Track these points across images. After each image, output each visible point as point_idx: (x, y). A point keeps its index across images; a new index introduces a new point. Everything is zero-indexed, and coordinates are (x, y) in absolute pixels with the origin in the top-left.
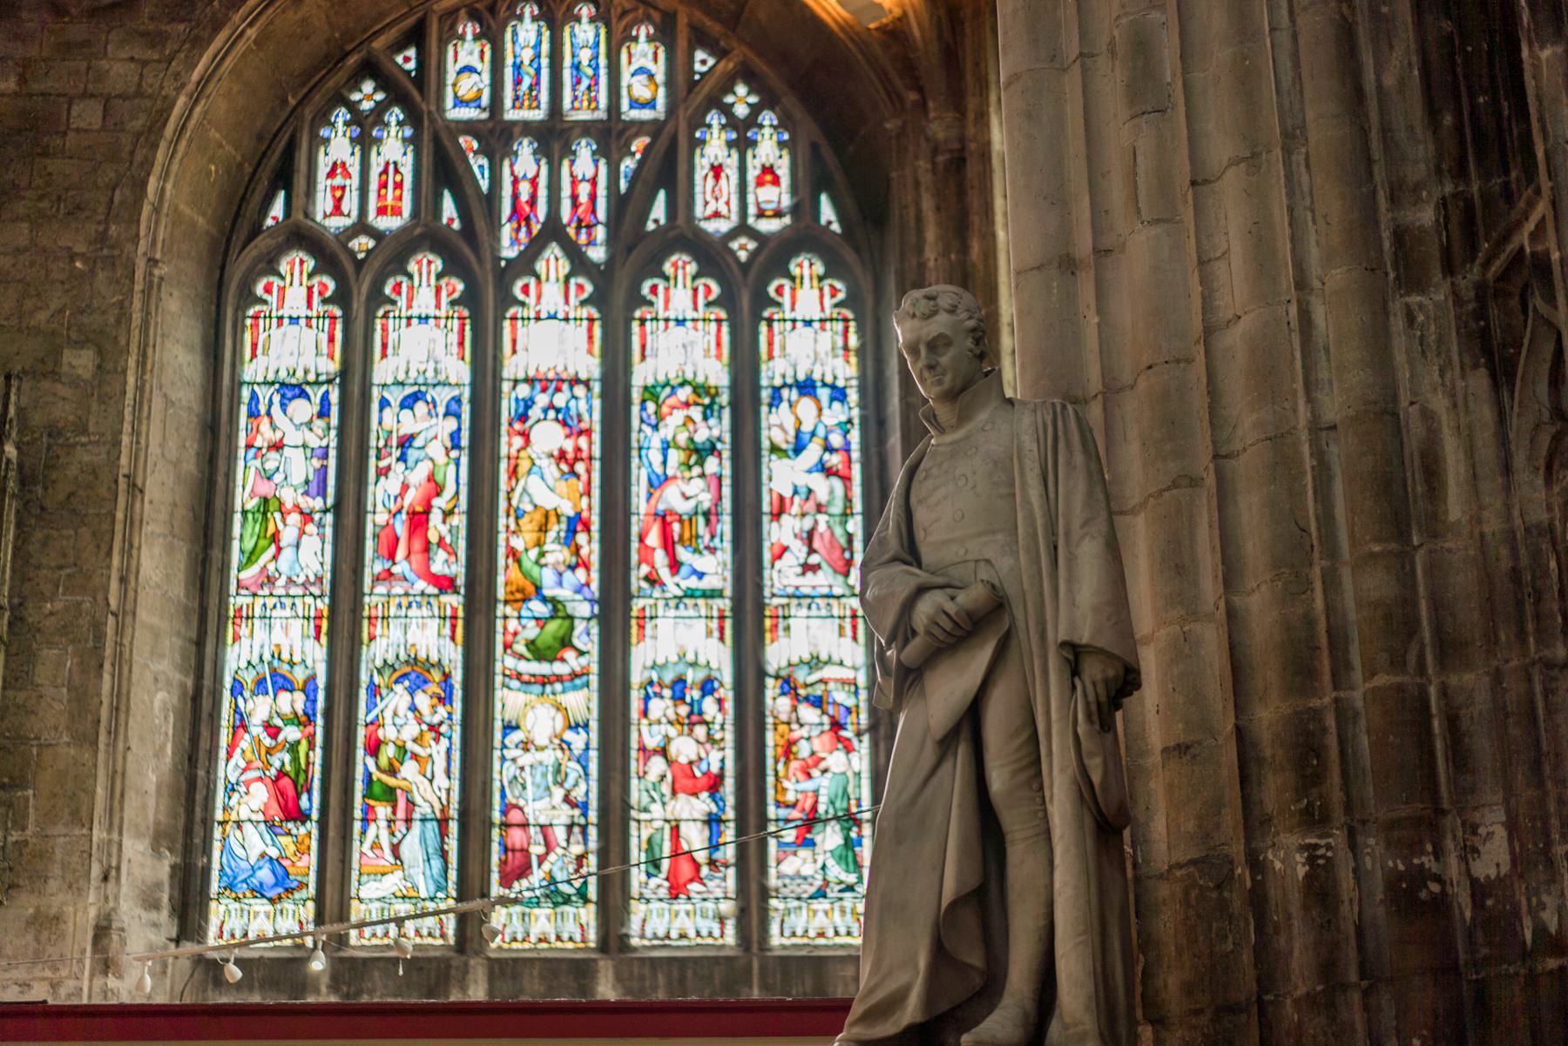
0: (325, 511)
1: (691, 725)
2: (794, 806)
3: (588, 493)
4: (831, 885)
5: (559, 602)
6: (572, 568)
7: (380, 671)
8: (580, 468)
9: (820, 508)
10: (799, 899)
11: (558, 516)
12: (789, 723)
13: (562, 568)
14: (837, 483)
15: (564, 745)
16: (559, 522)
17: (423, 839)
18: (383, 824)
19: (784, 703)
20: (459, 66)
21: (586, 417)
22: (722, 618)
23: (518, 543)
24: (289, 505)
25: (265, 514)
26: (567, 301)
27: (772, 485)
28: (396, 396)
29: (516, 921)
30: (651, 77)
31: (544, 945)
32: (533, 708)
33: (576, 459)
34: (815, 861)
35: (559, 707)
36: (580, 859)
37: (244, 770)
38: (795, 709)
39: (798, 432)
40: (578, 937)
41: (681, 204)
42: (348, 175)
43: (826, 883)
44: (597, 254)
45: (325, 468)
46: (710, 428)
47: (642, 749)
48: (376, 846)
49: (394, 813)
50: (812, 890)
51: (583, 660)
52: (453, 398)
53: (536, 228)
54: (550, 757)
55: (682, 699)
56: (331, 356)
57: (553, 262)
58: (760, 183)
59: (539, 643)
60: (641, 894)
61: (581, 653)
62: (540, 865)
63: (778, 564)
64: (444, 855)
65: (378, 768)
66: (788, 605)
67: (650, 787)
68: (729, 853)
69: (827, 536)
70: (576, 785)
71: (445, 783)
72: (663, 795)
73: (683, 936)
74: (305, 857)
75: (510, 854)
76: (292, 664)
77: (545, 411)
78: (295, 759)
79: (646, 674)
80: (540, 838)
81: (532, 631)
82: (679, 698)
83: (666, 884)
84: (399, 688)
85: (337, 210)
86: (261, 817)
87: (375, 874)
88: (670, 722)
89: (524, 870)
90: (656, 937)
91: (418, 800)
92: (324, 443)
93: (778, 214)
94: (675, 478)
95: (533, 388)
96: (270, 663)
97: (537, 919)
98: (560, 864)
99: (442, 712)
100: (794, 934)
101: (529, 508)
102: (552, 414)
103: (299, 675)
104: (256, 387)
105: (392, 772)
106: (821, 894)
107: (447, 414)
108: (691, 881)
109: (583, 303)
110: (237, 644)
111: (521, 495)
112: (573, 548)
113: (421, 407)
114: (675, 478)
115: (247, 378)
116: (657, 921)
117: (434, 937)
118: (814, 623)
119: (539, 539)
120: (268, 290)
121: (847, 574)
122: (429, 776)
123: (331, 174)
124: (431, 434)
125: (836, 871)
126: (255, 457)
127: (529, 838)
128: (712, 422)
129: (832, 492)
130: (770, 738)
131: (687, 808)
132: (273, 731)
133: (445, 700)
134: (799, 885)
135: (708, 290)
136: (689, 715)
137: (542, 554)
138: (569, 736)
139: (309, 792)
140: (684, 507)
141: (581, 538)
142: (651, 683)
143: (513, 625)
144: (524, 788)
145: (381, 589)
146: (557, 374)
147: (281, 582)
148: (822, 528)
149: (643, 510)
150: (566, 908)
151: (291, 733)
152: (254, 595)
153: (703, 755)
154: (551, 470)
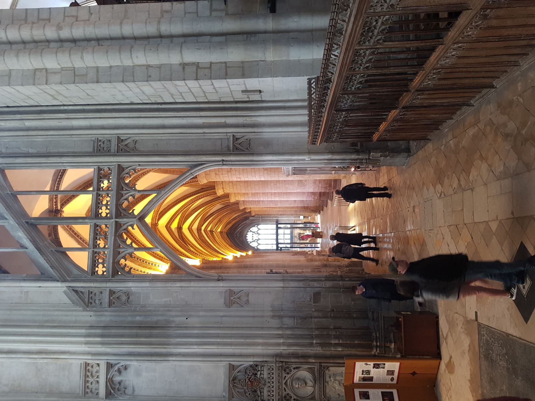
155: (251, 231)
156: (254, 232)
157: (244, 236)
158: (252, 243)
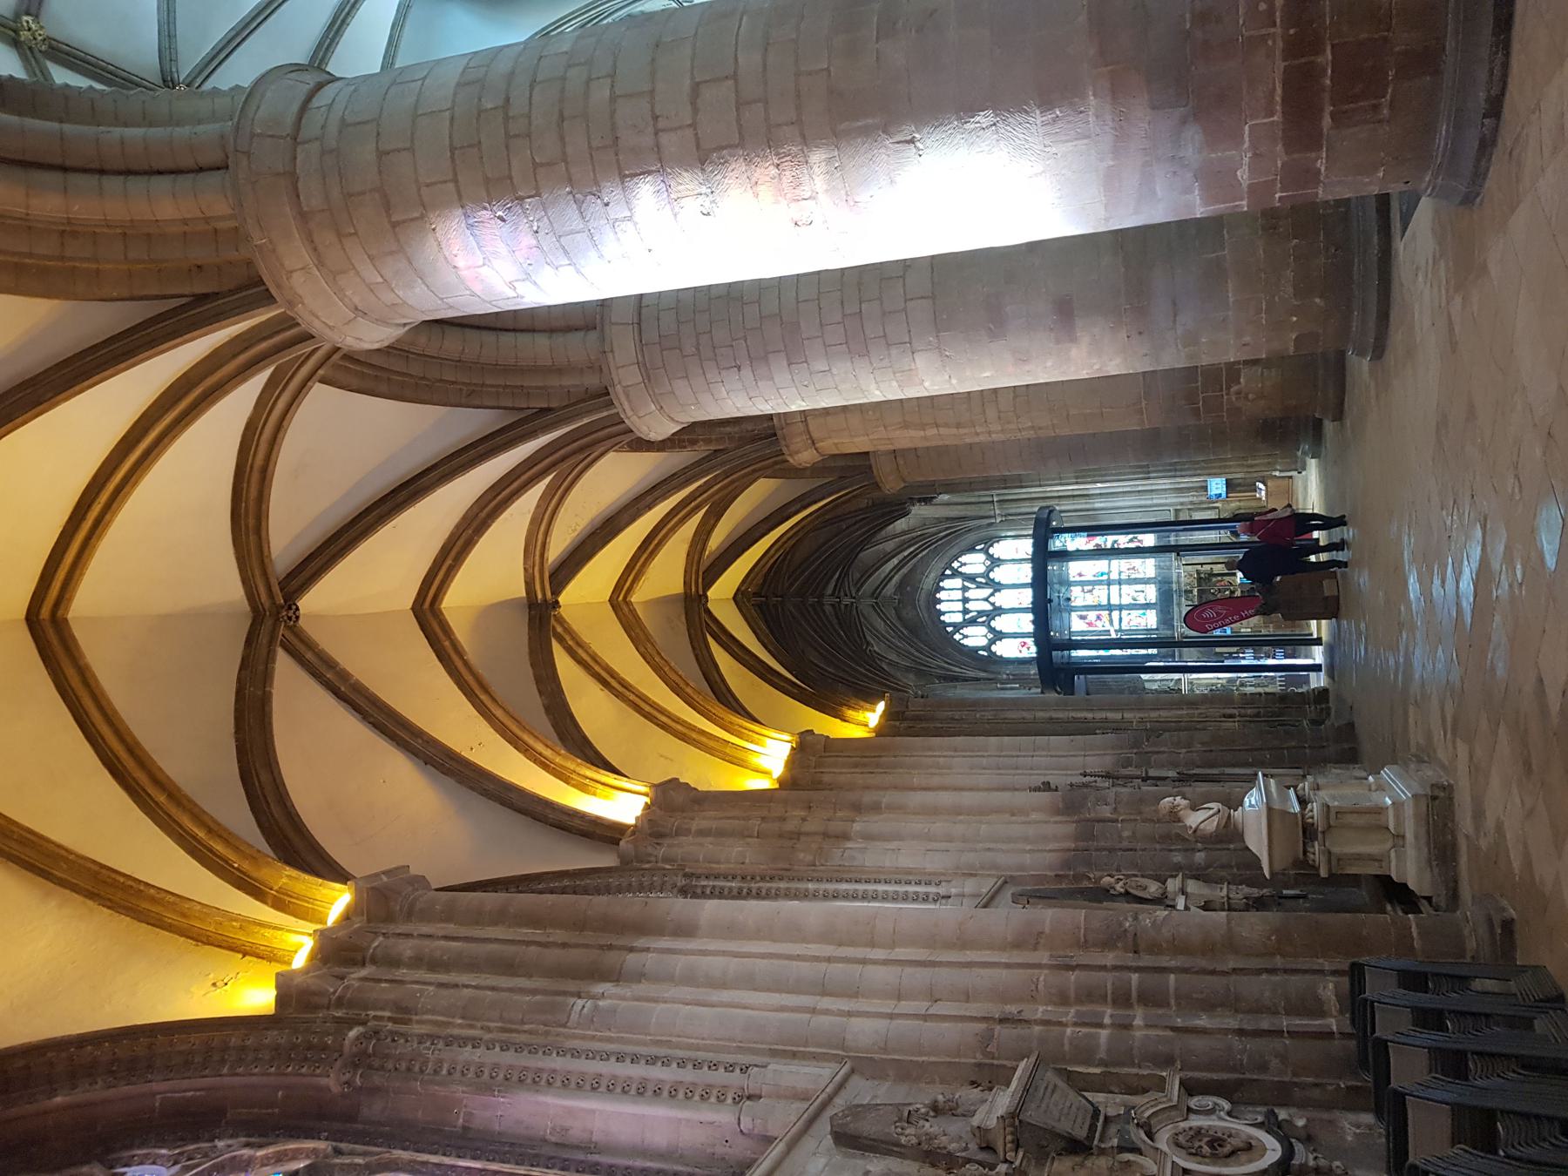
41: (981, 575)
57: (991, 599)
155: (956, 574)
156: (971, 578)
157: (922, 597)
158: (965, 631)
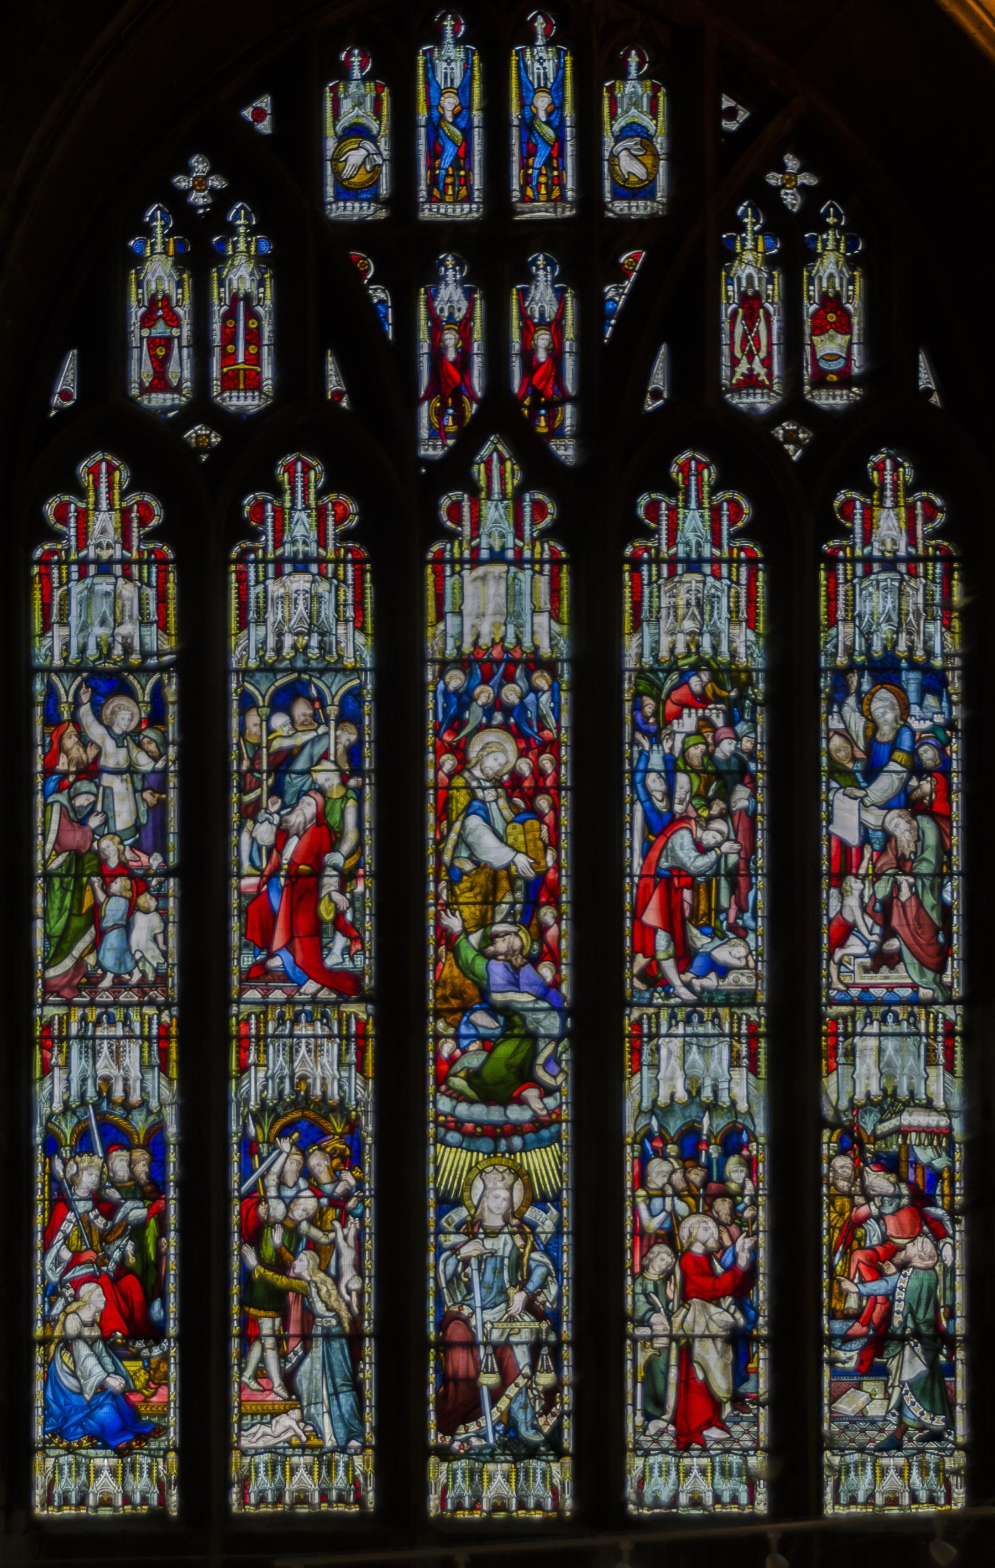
0: (166, 873)
1: (710, 1200)
2: (855, 1316)
3: (554, 842)
4: (911, 1431)
5: (516, 1012)
6: (534, 961)
7: (257, 1122)
8: (543, 803)
9: (903, 864)
10: (861, 1450)
11: (512, 879)
12: (850, 1196)
13: (519, 961)
14: (927, 824)
15: (526, 1229)
16: (513, 890)
17: (327, 1364)
18: (270, 1342)
19: (843, 1164)
20: (344, 122)
21: (551, 721)
22: (753, 1037)
23: (454, 923)
24: (113, 863)
25: (77, 877)
26: (519, 534)
27: (831, 828)
28: (262, 689)
29: (462, 1485)
30: (646, 138)
31: (502, 1515)
32: (481, 1172)
33: (539, 789)
34: (888, 1397)
35: (519, 1173)
36: (551, 1394)
37: (71, 1265)
38: (859, 1174)
39: (871, 741)
40: (549, 1504)
42: (174, 321)
43: (902, 1428)
44: (566, 451)
45: (161, 807)
46: (738, 739)
47: (639, 1232)
48: (261, 1373)
49: (285, 1324)
50: (881, 1438)
51: (551, 1102)
52: (349, 692)
53: (472, 409)
54: (503, 1245)
55: (695, 1158)
56: (162, 625)
58: (819, 329)
59: (486, 1072)
60: (636, 1442)
61: (547, 1091)
62: (494, 1402)
63: (838, 954)
64: (357, 1387)
65: (261, 1261)
66: (853, 1015)
67: (650, 1287)
68: (761, 1384)
69: (912, 911)
70: (544, 1285)
71: (356, 1285)
72: (668, 1301)
73: (696, 1502)
74: (163, 1391)
75: (451, 1385)
76: (127, 1107)
77: (488, 711)
78: (140, 1249)
79: (643, 1122)
80: (493, 1362)
81: (474, 1060)
82: (689, 1156)
83: (671, 1428)
84: (285, 1145)
85: (161, 383)
86: (96, 1332)
87: (263, 1415)
88: (677, 1194)
89: (473, 1411)
90: (656, 1503)
91: (320, 1307)
92: (160, 765)
93: (845, 380)
94: (685, 818)
95: (469, 675)
96: (96, 1106)
97: (490, 1479)
98: (521, 1399)
99: (349, 1178)
100: (853, 1501)
101: (468, 866)
102: (498, 717)
103: (140, 1122)
104: (55, 678)
105: (281, 1265)
106: (894, 1444)
107: (340, 720)
108: (708, 1425)
109: (545, 535)
110: (47, 1078)
111: (456, 847)
112: (534, 929)
113: (302, 709)
114: (685, 818)
115: (40, 661)
116: (661, 1481)
117: (347, 1503)
118: (890, 1045)
119: (484, 915)
120: (62, 515)
121: (940, 969)
122: (333, 1271)
123: (147, 320)
124: (319, 750)
125: (916, 1411)
126: (59, 790)
127: (477, 1363)
128: (741, 728)
129: (919, 838)
130: (828, 1217)
131: (702, 1320)
132: (107, 1208)
133: (353, 1160)
134: (863, 1431)
135: (736, 511)
136: (707, 1181)
137: (490, 939)
138: (532, 1214)
139: (635, 1427)
140: (697, 863)
141: (547, 914)
142: (649, 1135)
143: (447, 1048)
144: (470, 1290)
145: (253, 995)
146: (506, 651)
147: (107, 982)
148: (905, 894)
149: (637, 870)
150: (533, 1463)
151: (135, 1211)
152: (69, 1004)
153: (727, 1241)
154: (500, 809)
